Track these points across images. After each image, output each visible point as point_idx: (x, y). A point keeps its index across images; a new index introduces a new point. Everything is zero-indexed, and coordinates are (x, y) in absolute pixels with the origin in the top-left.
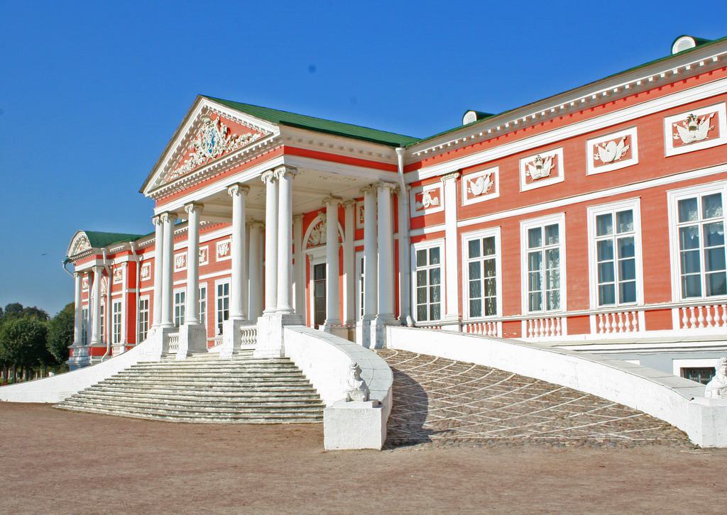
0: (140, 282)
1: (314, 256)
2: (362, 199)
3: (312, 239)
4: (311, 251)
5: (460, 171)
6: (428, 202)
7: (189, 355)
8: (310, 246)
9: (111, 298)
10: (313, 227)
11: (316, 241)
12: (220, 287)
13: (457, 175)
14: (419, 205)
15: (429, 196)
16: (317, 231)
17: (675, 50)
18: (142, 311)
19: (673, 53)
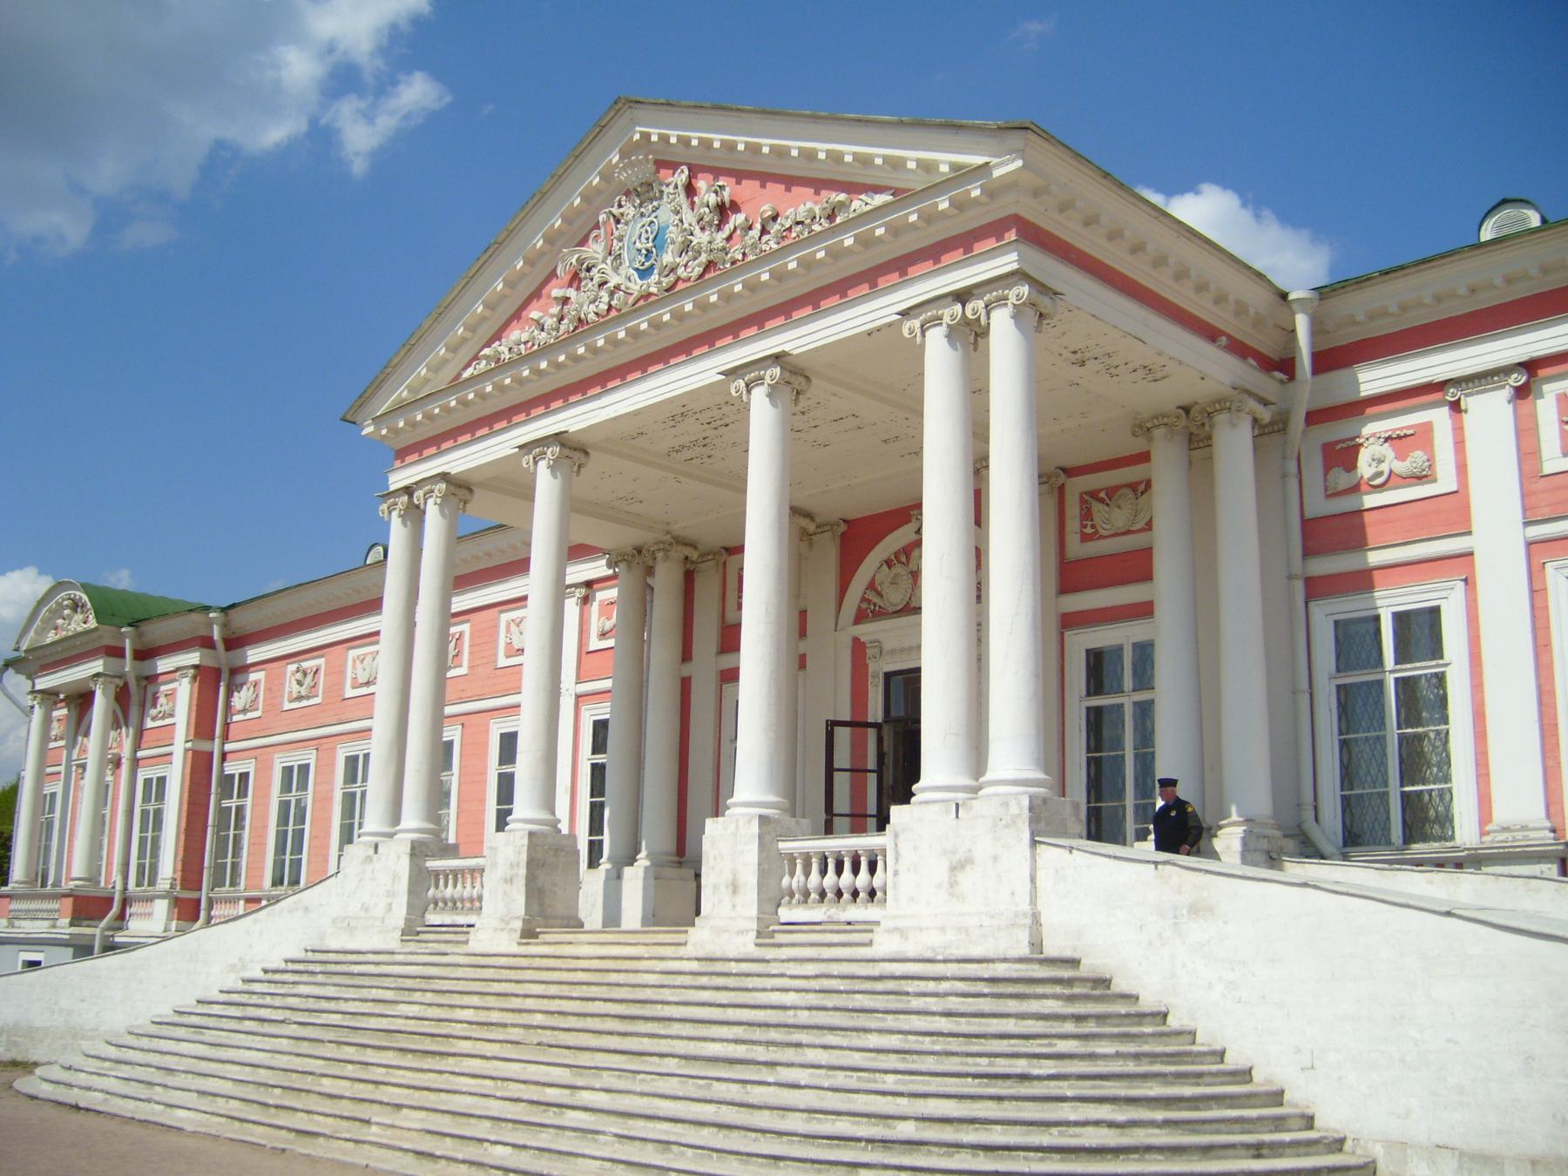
0: (227, 725)
1: (887, 646)
2: (1144, 457)
3: (880, 595)
4: (867, 631)
5: (1531, 366)
6: (1385, 467)
7: (529, 934)
8: (860, 618)
9: (136, 763)
10: (885, 556)
11: (895, 598)
12: (288, 771)
13: (1519, 379)
14: (1341, 479)
15: (1387, 450)
16: (898, 569)
17: (1487, 234)
18: (226, 803)
19: (1482, 240)
